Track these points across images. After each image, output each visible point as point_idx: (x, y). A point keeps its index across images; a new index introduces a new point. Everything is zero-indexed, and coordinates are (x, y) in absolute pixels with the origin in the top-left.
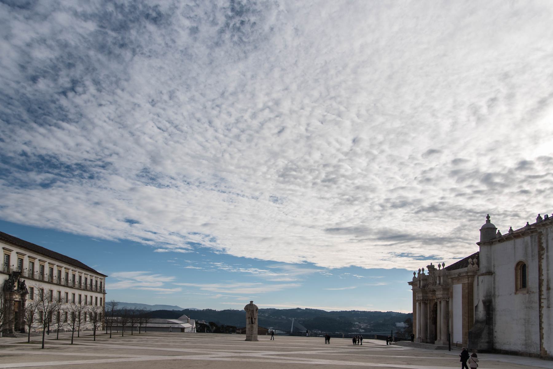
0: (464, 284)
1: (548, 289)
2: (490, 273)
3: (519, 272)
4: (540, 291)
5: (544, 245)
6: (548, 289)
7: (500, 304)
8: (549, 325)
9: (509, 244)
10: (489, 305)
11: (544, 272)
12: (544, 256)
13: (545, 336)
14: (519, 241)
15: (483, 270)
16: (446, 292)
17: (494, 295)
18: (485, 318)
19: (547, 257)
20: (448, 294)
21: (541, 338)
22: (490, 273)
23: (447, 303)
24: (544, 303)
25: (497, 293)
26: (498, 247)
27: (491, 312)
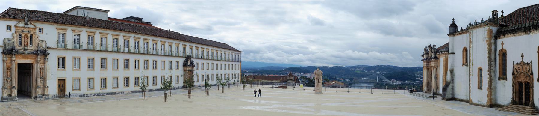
2: (453, 53)
3: (464, 53)
7: (457, 73)
10: (452, 72)
11: (471, 55)
21: (470, 92)
23: (437, 69)
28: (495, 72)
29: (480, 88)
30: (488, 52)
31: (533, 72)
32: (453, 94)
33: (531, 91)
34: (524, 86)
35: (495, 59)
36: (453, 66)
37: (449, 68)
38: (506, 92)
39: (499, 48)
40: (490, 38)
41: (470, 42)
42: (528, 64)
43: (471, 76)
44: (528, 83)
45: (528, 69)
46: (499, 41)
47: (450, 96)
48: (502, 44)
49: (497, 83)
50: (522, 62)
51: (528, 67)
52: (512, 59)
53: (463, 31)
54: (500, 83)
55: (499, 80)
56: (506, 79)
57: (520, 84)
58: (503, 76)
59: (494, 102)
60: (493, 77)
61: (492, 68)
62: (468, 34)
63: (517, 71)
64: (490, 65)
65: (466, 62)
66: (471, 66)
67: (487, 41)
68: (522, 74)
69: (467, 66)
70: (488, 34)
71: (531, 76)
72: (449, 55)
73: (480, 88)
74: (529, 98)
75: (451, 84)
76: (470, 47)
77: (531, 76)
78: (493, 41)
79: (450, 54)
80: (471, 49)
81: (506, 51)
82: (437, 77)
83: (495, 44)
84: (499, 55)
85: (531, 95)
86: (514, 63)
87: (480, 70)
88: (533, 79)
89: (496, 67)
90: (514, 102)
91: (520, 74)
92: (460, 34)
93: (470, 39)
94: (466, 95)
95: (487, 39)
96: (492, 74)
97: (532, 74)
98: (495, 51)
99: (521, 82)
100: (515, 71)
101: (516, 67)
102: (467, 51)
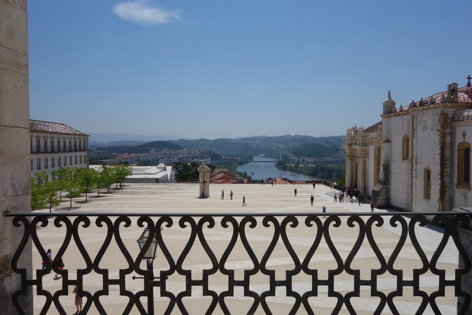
0: (375, 147)
1: (416, 163)
2: (388, 141)
5: (415, 126)
6: (416, 163)
8: (416, 191)
9: (399, 119)
10: (387, 169)
11: (414, 149)
12: (415, 136)
14: (405, 117)
15: (384, 139)
17: (391, 160)
18: (383, 179)
19: (416, 136)
22: (388, 141)
23: (365, 161)
24: (414, 175)
25: (392, 159)
26: (394, 120)
28: (451, 176)
29: (427, 196)
30: (439, 147)
37: (382, 162)
39: (459, 139)
40: (444, 126)
43: (414, 178)
48: (464, 135)
49: (454, 192)
53: (402, 112)
61: (447, 170)
65: (407, 156)
66: (414, 165)
67: (438, 131)
70: (439, 121)
73: (427, 196)
80: (414, 139)
83: (452, 134)
84: (458, 150)
92: (399, 115)
93: (413, 125)
96: (447, 179)
102: (408, 140)
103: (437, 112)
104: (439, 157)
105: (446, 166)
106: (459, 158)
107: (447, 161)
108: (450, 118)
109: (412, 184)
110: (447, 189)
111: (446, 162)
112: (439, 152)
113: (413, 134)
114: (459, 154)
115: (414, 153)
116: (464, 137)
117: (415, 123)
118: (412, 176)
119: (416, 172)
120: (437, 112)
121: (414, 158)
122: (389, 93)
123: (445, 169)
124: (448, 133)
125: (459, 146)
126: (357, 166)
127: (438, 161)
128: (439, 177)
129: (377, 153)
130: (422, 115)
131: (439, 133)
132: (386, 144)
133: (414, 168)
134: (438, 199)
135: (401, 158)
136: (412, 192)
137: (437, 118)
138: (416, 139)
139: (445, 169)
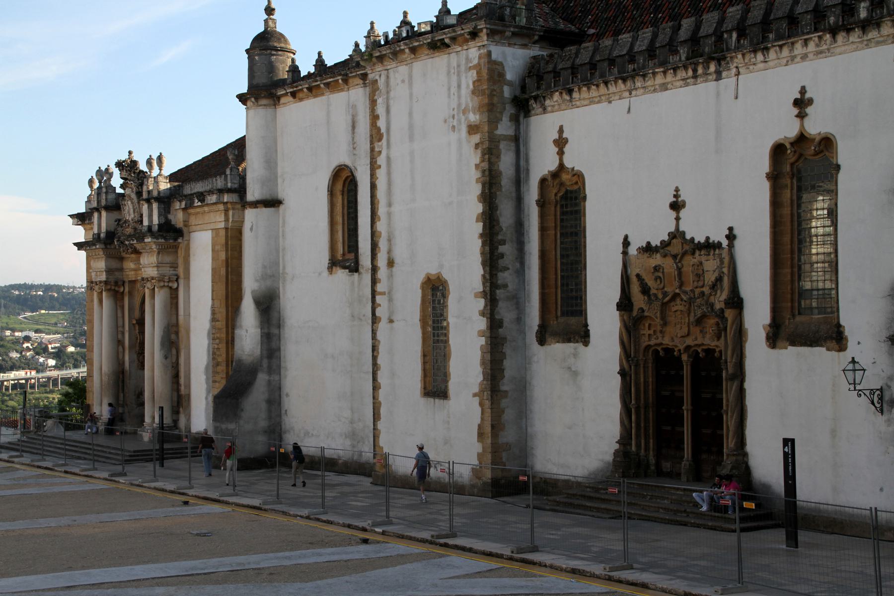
0: (215, 231)
1: (391, 263)
2: (273, 203)
4: (374, 269)
5: (381, 124)
6: (391, 263)
7: (296, 307)
10: (268, 305)
11: (382, 211)
13: (383, 411)
16: (168, 259)
18: (258, 352)
19: (388, 159)
20: (174, 266)
21: (376, 416)
23: (174, 295)
25: (289, 270)
27: (275, 331)
28: (518, 301)
30: (477, 189)
31: (745, 291)
32: (275, 430)
33: (728, 396)
34: (686, 372)
35: (520, 226)
36: (273, 274)
37: (250, 284)
38: (581, 410)
39: (543, 162)
40: (491, 109)
41: (376, 135)
42: (709, 246)
43: (382, 326)
44: (709, 352)
45: (710, 278)
46: (543, 126)
47: (259, 446)
48: (561, 143)
50: (677, 235)
51: (710, 265)
52: (618, 224)
54: (548, 364)
55: (542, 341)
56: (583, 336)
57: (666, 362)
58: (565, 318)
59: (513, 467)
60: (508, 328)
61: (506, 277)
62: (357, 94)
63: (645, 290)
64: (492, 261)
65: (345, 256)
66: (382, 273)
67: (472, 129)
68: (678, 306)
69: (354, 268)
71: (729, 314)
72: (250, 215)
73: (435, 386)
74: (717, 442)
75: (262, 378)
76: (374, 167)
77: (729, 314)
78: (505, 128)
79: (255, 204)
80: (381, 174)
81: (579, 177)
82: (174, 340)
83: (518, 141)
85: (730, 421)
86: (626, 243)
87: (435, 290)
88: (740, 334)
89: (521, 272)
90: (627, 461)
91: (664, 306)
93: (374, 118)
94: (353, 435)
95: (474, 118)
96: (506, 312)
97: (736, 302)
98: (519, 180)
99: (668, 351)
100: (635, 288)
101: (641, 266)
103: (468, 60)
104: (479, 227)
105: (501, 263)
106: (543, 229)
107: (503, 242)
108: (510, 84)
109: (374, 348)
110: (507, 350)
111: (502, 249)
112: (479, 208)
113: (373, 156)
114: (542, 216)
115: (381, 226)
116: (561, 153)
117: (380, 110)
118: (375, 319)
119: (390, 300)
120: (468, 60)
121: (383, 245)
122: (269, 10)
123: (500, 275)
124: (506, 138)
125: (543, 181)
126: (141, 323)
127: (474, 245)
128: (481, 303)
129: (223, 256)
130: (410, 77)
131: (476, 138)
132: (265, 212)
133: (380, 288)
134: (476, 389)
135: (324, 258)
136: (375, 379)
137: (469, 79)
138: (389, 173)
139: (500, 275)
